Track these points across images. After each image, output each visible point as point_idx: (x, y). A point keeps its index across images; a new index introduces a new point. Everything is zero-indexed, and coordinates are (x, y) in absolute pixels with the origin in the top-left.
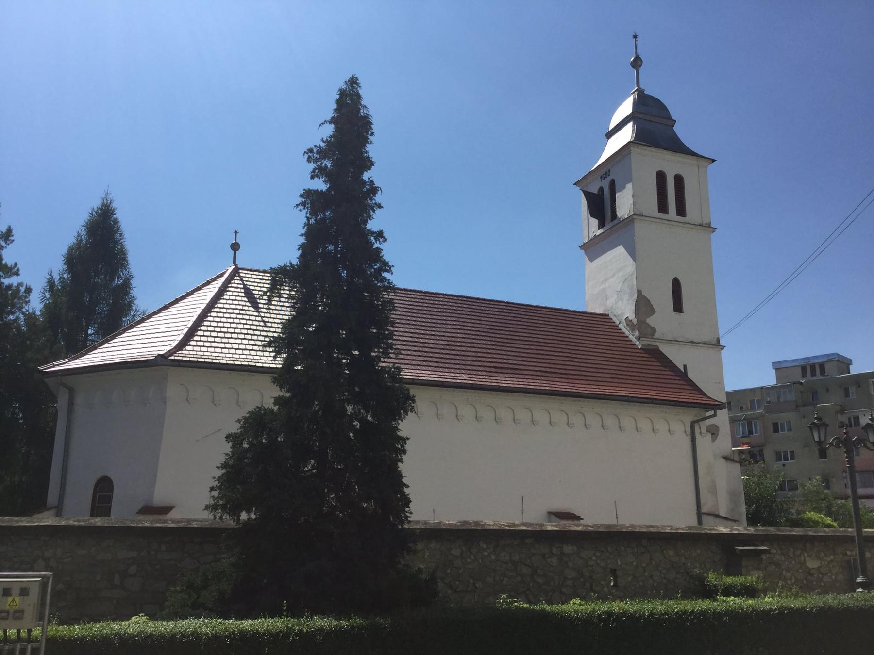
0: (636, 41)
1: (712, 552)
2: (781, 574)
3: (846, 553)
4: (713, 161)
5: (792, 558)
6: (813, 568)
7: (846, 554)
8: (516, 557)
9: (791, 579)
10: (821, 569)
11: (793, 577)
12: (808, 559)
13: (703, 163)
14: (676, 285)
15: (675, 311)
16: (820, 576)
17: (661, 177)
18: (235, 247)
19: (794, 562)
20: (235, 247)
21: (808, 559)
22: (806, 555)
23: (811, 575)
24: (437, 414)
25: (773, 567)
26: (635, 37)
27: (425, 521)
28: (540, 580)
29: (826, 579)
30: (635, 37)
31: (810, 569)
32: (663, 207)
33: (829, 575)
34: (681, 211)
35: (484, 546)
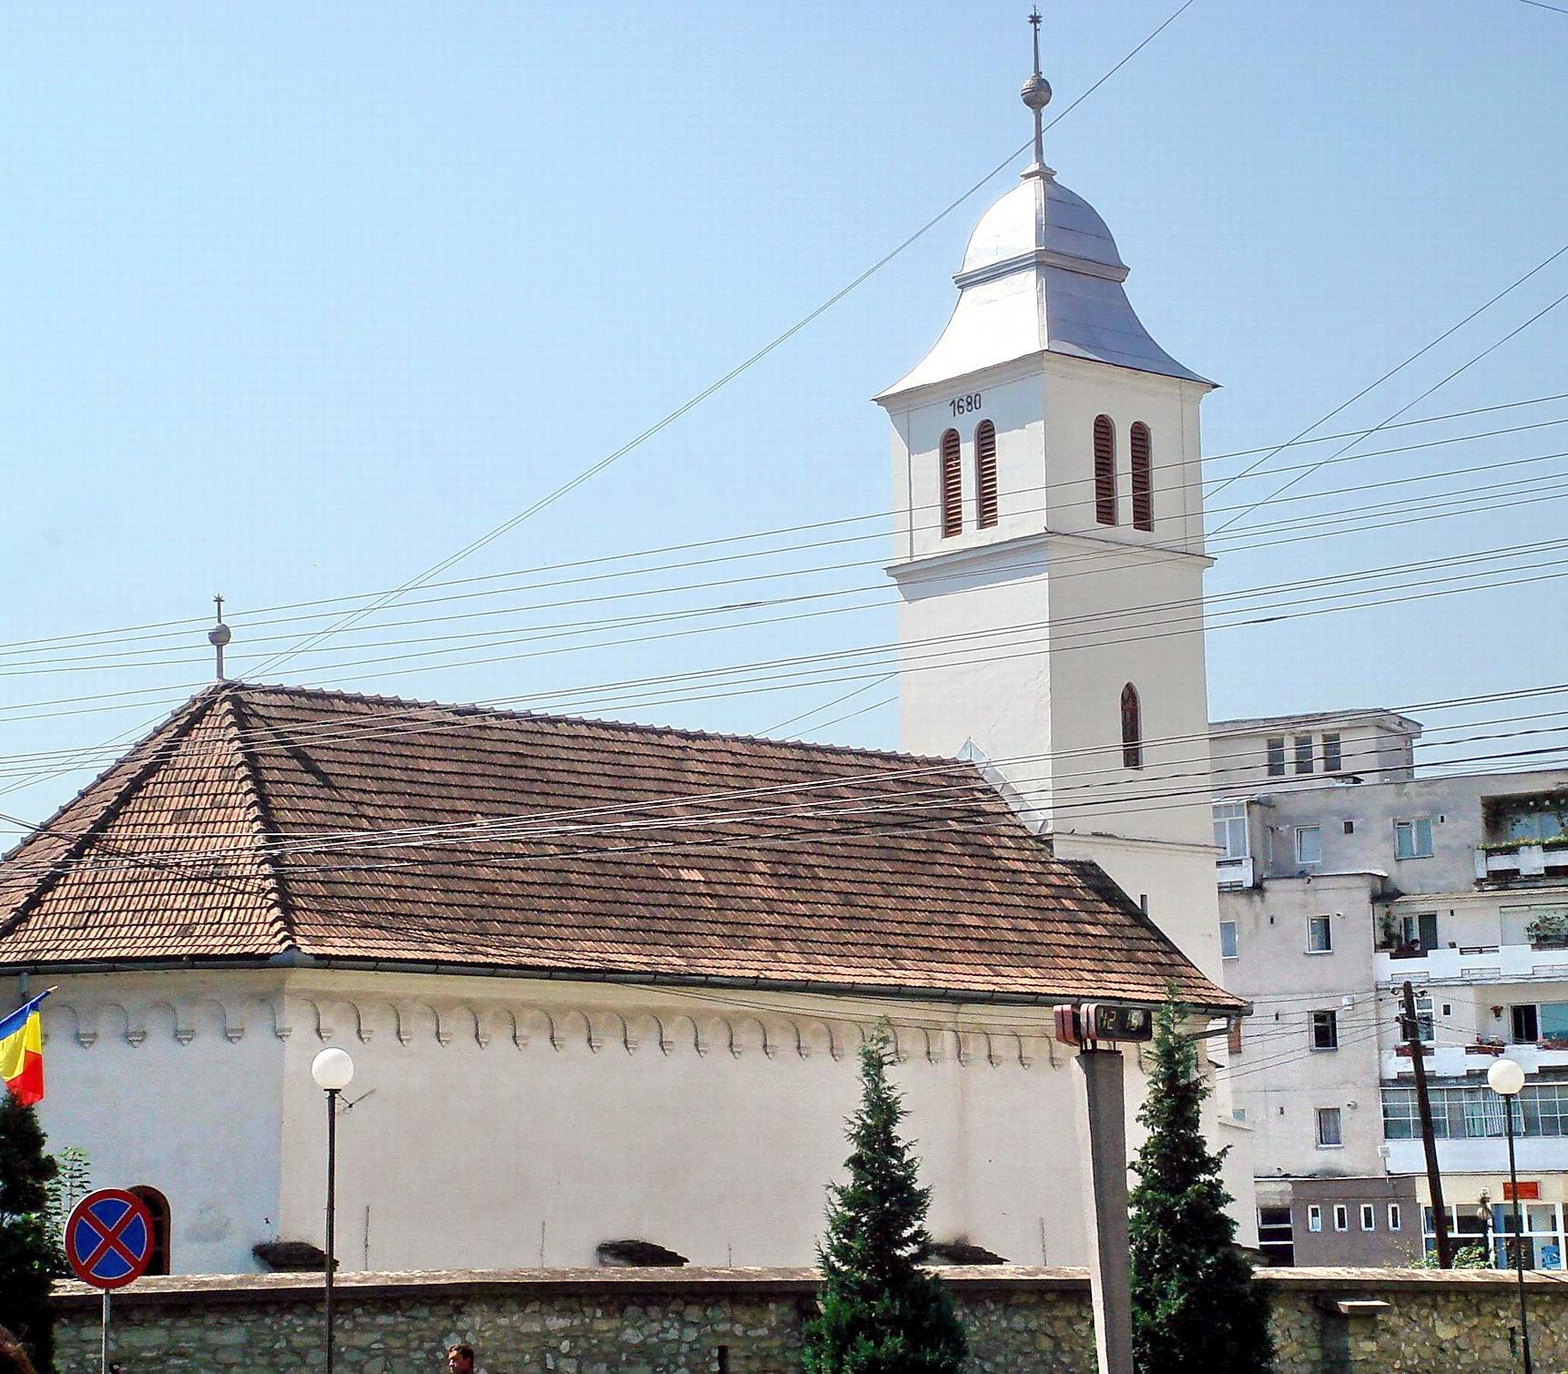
0: (1036, 30)
1: (1299, 1311)
2: (1399, 1348)
3: (1497, 1313)
4: (1216, 386)
5: (1415, 1321)
6: (1446, 1341)
7: (1498, 1316)
8: (1033, 1325)
9: (1412, 1359)
10: (1457, 1341)
11: (1416, 1356)
12: (1439, 1323)
13: (1190, 390)
14: (1130, 700)
15: (1127, 764)
16: (1457, 1352)
17: (1103, 429)
18: (220, 637)
19: (1417, 1329)
20: (220, 637)
21: (1439, 1323)
22: (1435, 1315)
23: (1442, 1350)
24: (731, 1044)
25: (1388, 1337)
26: (1035, 20)
27: (699, 1268)
28: (1066, 1360)
29: (1465, 1359)
30: (1035, 20)
31: (1442, 1342)
32: (1106, 513)
33: (1471, 1351)
34: (1143, 517)
35: (992, 1307)
